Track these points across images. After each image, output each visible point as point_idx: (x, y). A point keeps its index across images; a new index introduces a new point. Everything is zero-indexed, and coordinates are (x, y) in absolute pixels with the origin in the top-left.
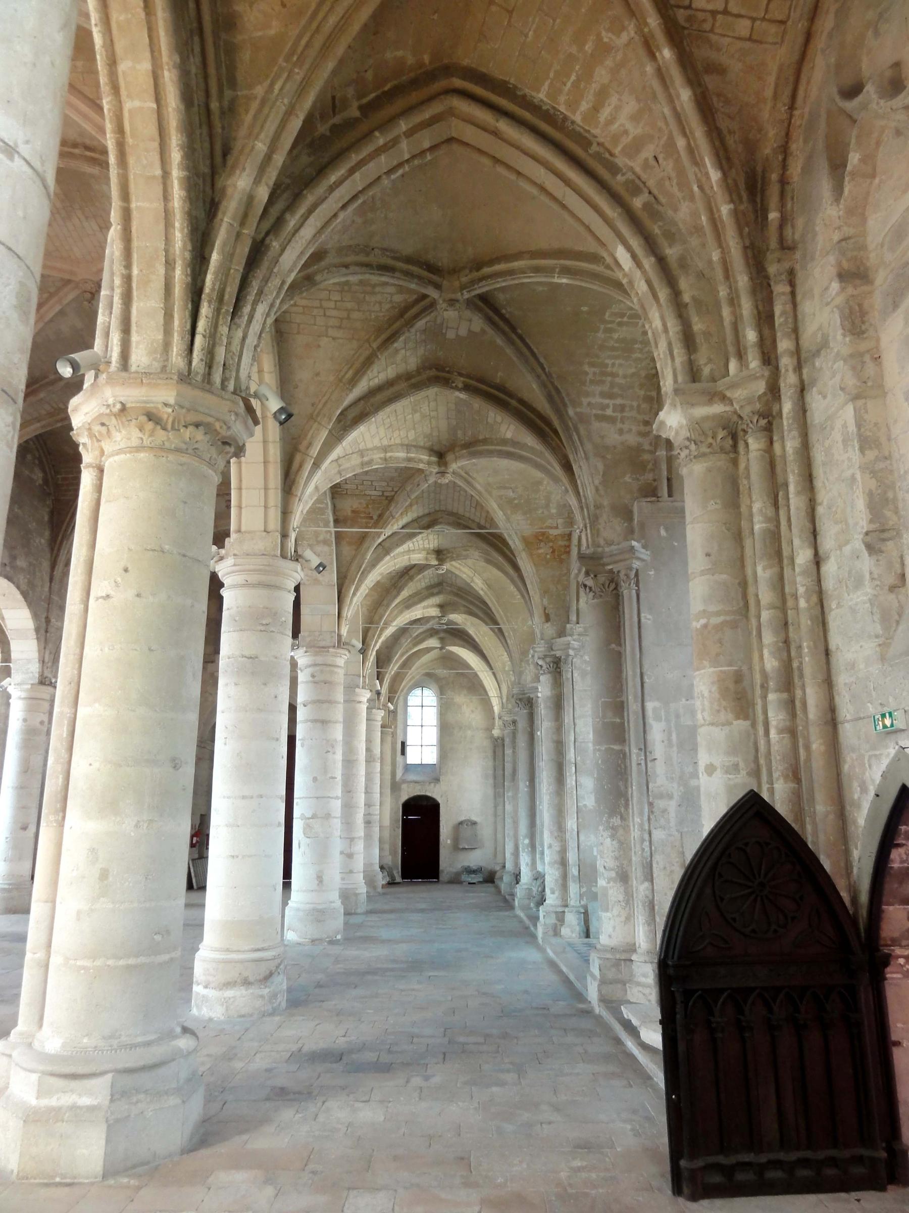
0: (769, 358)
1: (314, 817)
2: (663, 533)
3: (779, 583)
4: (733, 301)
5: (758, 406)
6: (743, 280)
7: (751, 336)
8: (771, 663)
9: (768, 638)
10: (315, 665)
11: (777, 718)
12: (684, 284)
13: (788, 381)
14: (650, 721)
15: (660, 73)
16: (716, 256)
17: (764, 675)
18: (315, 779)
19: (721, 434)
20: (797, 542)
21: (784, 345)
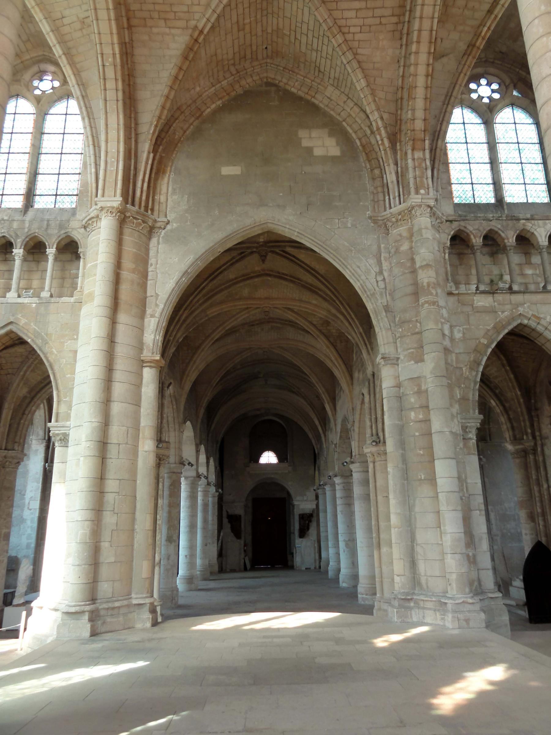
0: (534, 437)
1: (349, 540)
2: (489, 452)
3: (540, 491)
4: (524, 421)
5: (532, 448)
6: (526, 417)
7: (529, 431)
8: (539, 510)
9: (538, 504)
10: (344, 483)
11: (541, 523)
12: (510, 413)
13: (539, 442)
14: (490, 512)
15: (506, 371)
16: (519, 410)
17: (538, 513)
18: (348, 526)
19: (523, 453)
20: (544, 482)
21: (537, 434)
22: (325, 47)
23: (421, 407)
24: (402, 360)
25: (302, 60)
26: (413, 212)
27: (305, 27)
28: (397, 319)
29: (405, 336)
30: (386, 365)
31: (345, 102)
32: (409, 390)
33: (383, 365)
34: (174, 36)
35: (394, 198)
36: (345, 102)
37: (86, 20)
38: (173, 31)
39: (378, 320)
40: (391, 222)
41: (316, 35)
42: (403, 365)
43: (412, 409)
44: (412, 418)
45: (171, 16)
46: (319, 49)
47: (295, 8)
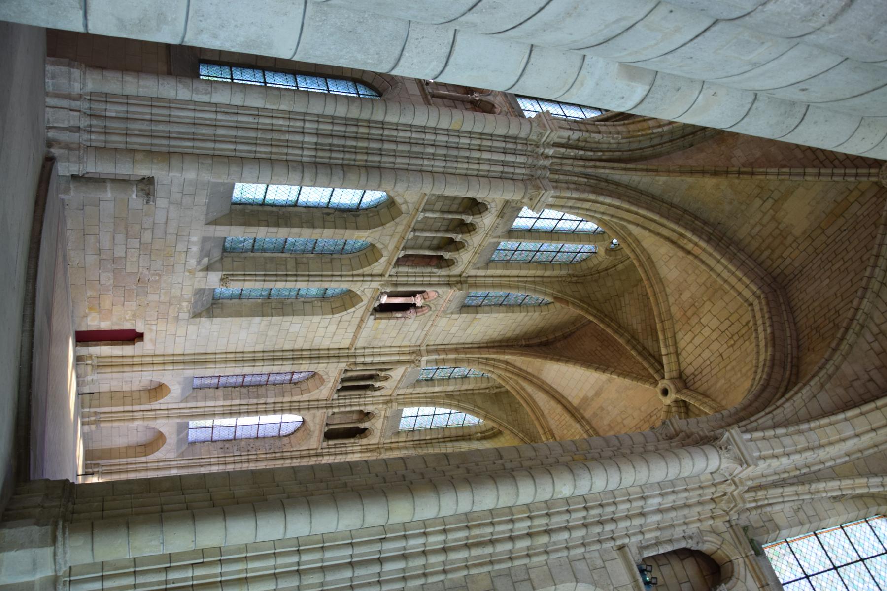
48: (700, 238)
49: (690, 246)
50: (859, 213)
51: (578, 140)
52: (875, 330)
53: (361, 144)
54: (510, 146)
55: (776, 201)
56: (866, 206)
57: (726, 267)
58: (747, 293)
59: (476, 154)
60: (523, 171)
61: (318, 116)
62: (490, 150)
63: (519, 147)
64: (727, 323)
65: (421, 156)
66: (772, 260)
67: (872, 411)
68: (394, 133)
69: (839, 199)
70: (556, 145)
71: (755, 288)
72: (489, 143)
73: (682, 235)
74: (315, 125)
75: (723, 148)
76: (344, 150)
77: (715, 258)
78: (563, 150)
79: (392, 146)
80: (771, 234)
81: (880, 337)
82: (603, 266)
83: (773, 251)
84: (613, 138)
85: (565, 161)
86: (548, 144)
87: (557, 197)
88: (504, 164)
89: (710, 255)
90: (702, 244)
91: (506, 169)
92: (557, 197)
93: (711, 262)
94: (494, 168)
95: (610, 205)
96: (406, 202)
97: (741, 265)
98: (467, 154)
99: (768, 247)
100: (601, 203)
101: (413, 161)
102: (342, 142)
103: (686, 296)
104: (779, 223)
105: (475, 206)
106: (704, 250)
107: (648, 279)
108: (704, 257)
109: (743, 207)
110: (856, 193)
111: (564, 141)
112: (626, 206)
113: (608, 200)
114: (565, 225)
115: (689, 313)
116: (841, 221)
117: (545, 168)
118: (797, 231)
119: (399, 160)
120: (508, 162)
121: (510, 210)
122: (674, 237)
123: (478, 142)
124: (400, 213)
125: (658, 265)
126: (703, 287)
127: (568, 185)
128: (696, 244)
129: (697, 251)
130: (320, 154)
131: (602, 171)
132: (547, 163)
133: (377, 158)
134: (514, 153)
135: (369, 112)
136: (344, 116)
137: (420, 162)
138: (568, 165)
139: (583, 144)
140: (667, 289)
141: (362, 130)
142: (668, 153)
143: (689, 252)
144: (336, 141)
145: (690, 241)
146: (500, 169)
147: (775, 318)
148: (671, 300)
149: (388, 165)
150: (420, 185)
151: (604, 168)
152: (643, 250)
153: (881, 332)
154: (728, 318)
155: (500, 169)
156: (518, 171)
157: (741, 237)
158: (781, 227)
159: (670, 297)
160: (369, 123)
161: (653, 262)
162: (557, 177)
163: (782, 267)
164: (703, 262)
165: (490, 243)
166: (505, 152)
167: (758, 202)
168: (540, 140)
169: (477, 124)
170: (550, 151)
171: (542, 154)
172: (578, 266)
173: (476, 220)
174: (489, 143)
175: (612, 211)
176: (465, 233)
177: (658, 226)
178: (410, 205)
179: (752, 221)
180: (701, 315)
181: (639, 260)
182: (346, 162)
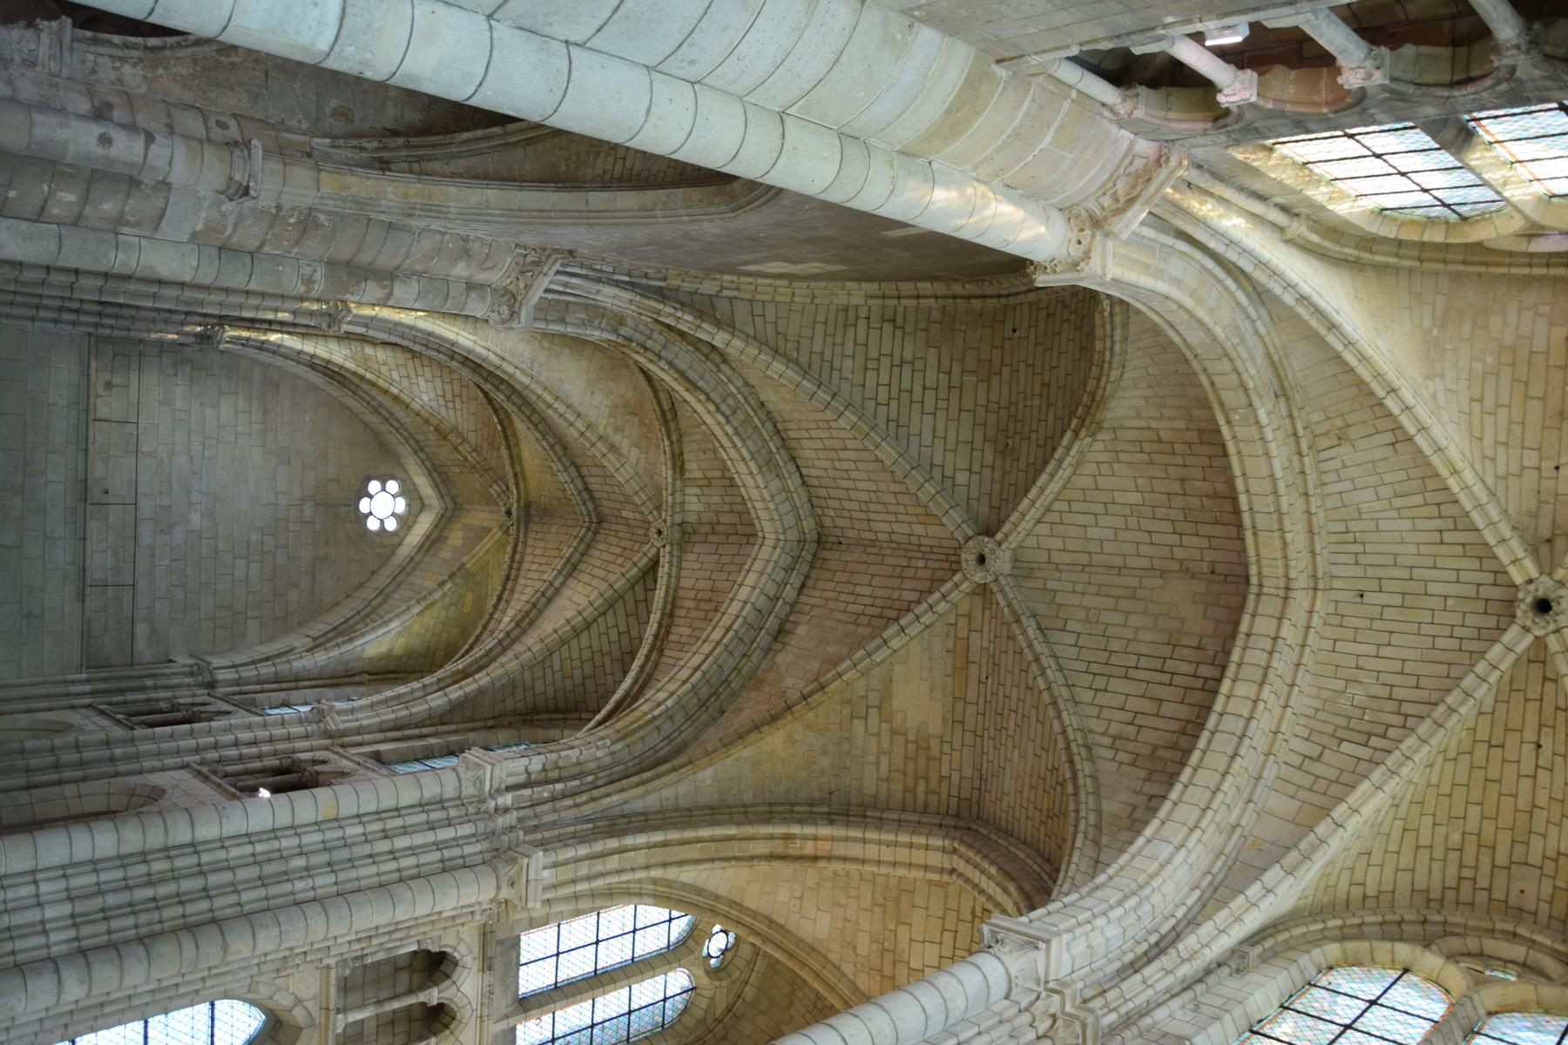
22: (884, 379)
23: (80, 216)
24: (222, 203)
25: (935, 329)
26: (505, 309)
27: (929, 407)
28: (322, 217)
29: (271, 226)
30: (228, 187)
31: (814, 297)
32: (135, 206)
33: (231, 178)
34: (1138, 416)
35: (566, 285)
36: (814, 297)
37: (1336, 442)
38: (1142, 423)
39: (344, 201)
40: (533, 263)
41: (905, 396)
42: (207, 203)
43: (85, 199)
44: (60, 195)
45: (1147, 447)
46: (896, 370)
47: (952, 435)
48: (815, 823)
49: (809, 848)
50: (985, 644)
51: (544, 770)
52: (1107, 741)
53: (163, 890)
54: (435, 816)
55: (879, 707)
56: (986, 629)
57: (880, 843)
58: (935, 859)
59: (384, 846)
60: (478, 848)
61: (63, 867)
62: (405, 831)
63: (453, 813)
64: (948, 937)
65: (286, 876)
66: (934, 792)
67: (1172, 810)
68: (222, 854)
69: (950, 645)
70: (509, 789)
71: (939, 843)
72: (398, 822)
73: (787, 838)
74: (62, 884)
75: (767, 689)
76: (132, 908)
77: (856, 840)
78: (527, 792)
79: (226, 877)
80: (906, 757)
81: (1118, 743)
82: (720, 1008)
83: (927, 779)
84: (598, 748)
85: (539, 809)
86: (498, 791)
87: (555, 865)
88: (439, 846)
89: (846, 839)
90: (825, 831)
91: (447, 854)
92: (555, 865)
93: (855, 850)
94: (424, 859)
95: (649, 847)
96: (299, 1001)
97: (900, 825)
98: (367, 849)
99: (916, 779)
100: (635, 849)
101: (274, 890)
102: (124, 897)
103: (863, 942)
104: (906, 734)
105: (435, 965)
106: (833, 839)
107: (791, 956)
108: (840, 849)
109: (846, 747)
110: (962, 623)
111: (522, 778)
112: (674, 835)
113: (641, 839)
114: (613, 954)
115: (887, 971)
116: (973, 670)
117: (511, 828)
118: (935, 727)
119: (246, 896)
120: (446, 841)
121: (500, 953)
122: (778, 847)
123: (377, 826)
124: (297, 1030)
125: (791, 927)
126: (877, 910)
127: (563, 841)
128: (816, 838)
129: (824, 847)
130: (86, 930)
131: (607, 801)
132: (511, 818)
133: (204, 905)
134: (449, 823)
135: (162, 831)
136: (113, 853)
137: (287, 887)
138: (547, 813)
139: (556, 774)
140: (832, 956)
141: (158, 866)
142: (695, 738)
143: (815, 858)
144: (112, 900)
145: (804, 838)
146: (436, 856)
147: (993, 855)
148: (848, 969)
149: (229, 912)
150: (302, 924)
151: (608, 795)
152: (755, 914)
153: (1115, 738)
154: (944, 930)
155: (436, 856)
156: (468, 850)
157: (873, 791)
158: (911, 737)
159: (843, 967)
160: (167, 851)
161: (782, 927)
162: (539, 836)
163: (954, 792)
164: (845, 859)
165: (496, 1036)
166: (432, 827)
167: (858, 725)
168: (481, 790)
169: (363, 796)
170: (507, 799)
171: (496, 810)
172: (679, 1027)
173: (447, 994)
174: (398, 822)
175: (659, 855)
176: (440, 1031)
177: (744, 844)
178: (310, 1005)
179: (871, 758)
180: (905, 957)
181: (757, 934)
182: (143, 931)
